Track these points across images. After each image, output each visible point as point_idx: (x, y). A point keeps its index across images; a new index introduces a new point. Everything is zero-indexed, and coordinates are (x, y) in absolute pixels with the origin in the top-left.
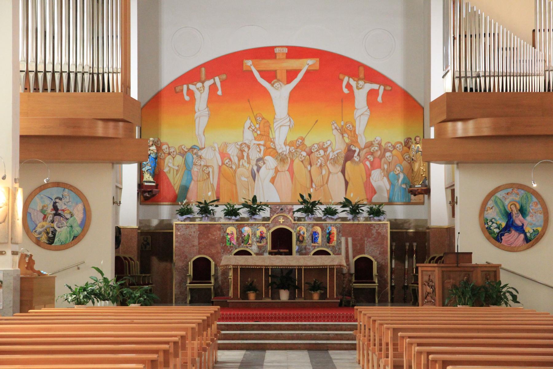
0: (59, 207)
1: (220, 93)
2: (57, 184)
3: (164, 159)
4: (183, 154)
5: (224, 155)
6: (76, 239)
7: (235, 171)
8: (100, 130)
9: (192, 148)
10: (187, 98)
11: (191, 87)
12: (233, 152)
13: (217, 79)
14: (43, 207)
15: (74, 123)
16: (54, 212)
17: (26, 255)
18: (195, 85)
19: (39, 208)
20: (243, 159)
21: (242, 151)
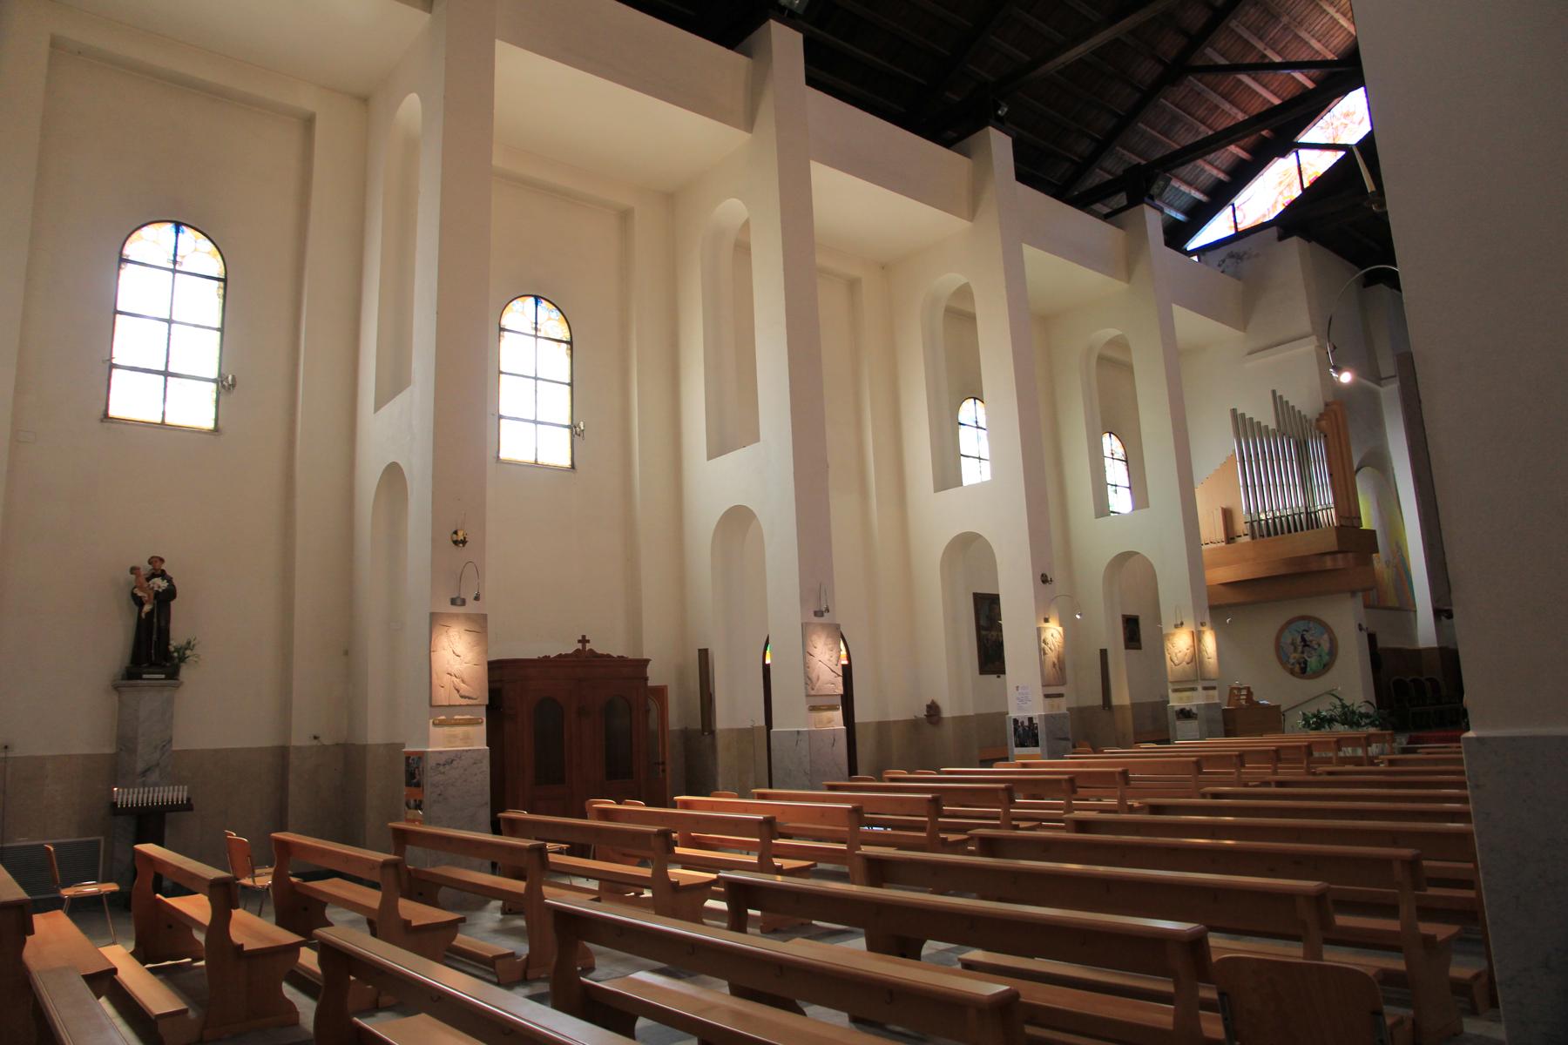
2: (1303, 618)
6: (1326, 667)
8: (1329, 563)
15: (1303, 560)
17: (1239, 689)
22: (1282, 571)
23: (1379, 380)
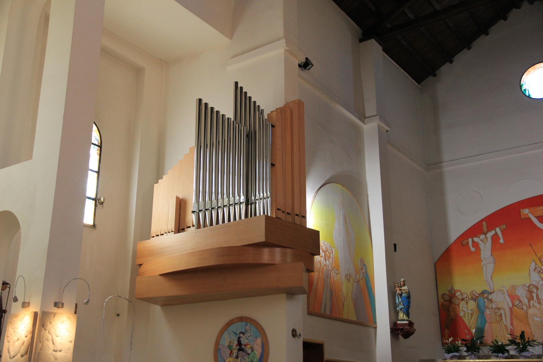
0: (242, 343)
1: (502, 241)
2: (241, 319)
3: (459, 305)
4: (475, 299)
5: (513, 297)
7: (527, 313)
9: (483, 293)
10: (473, 249)
11: (476, 239)
12: (521, 293)
13: (498, 229)
14: (230, 343)
16: (238, 347)
18: (479, 237)
19: (227, 344)
20: (533, 299)
21: (531, 292)
22: (212, 262)
23: (363, 117)
